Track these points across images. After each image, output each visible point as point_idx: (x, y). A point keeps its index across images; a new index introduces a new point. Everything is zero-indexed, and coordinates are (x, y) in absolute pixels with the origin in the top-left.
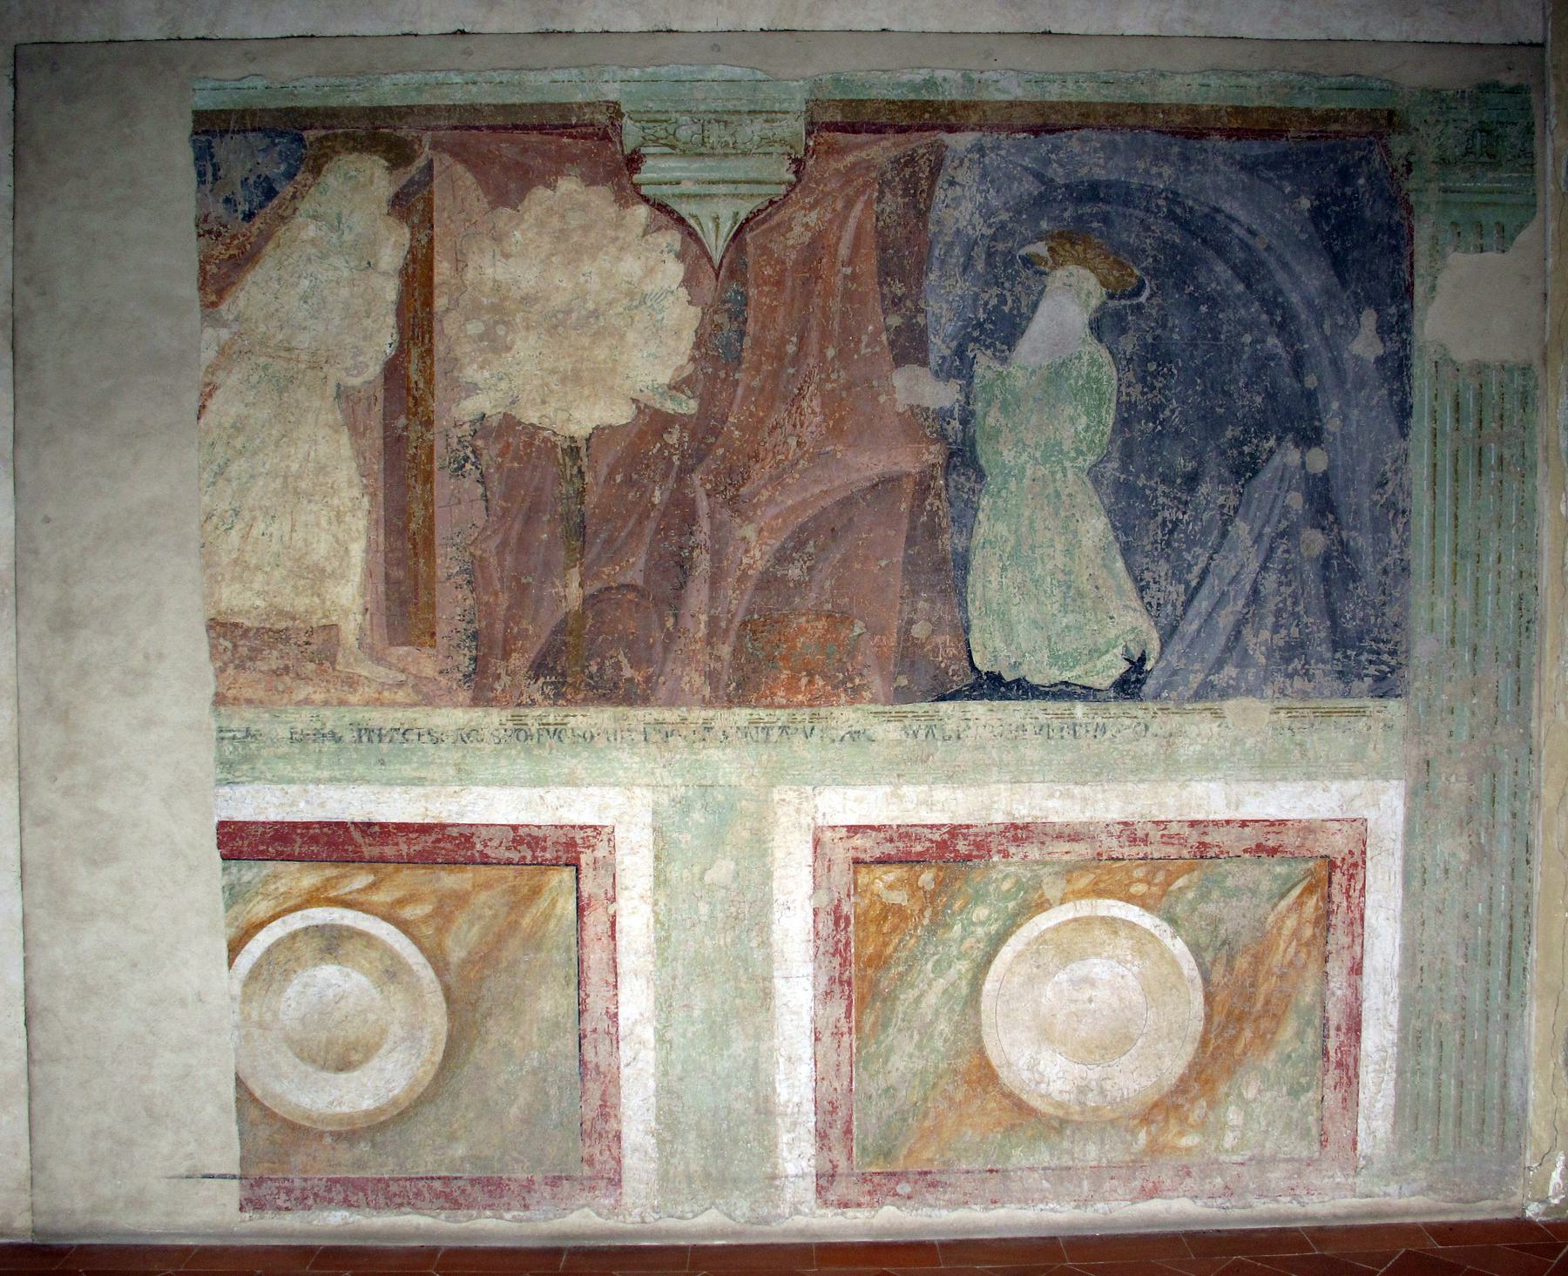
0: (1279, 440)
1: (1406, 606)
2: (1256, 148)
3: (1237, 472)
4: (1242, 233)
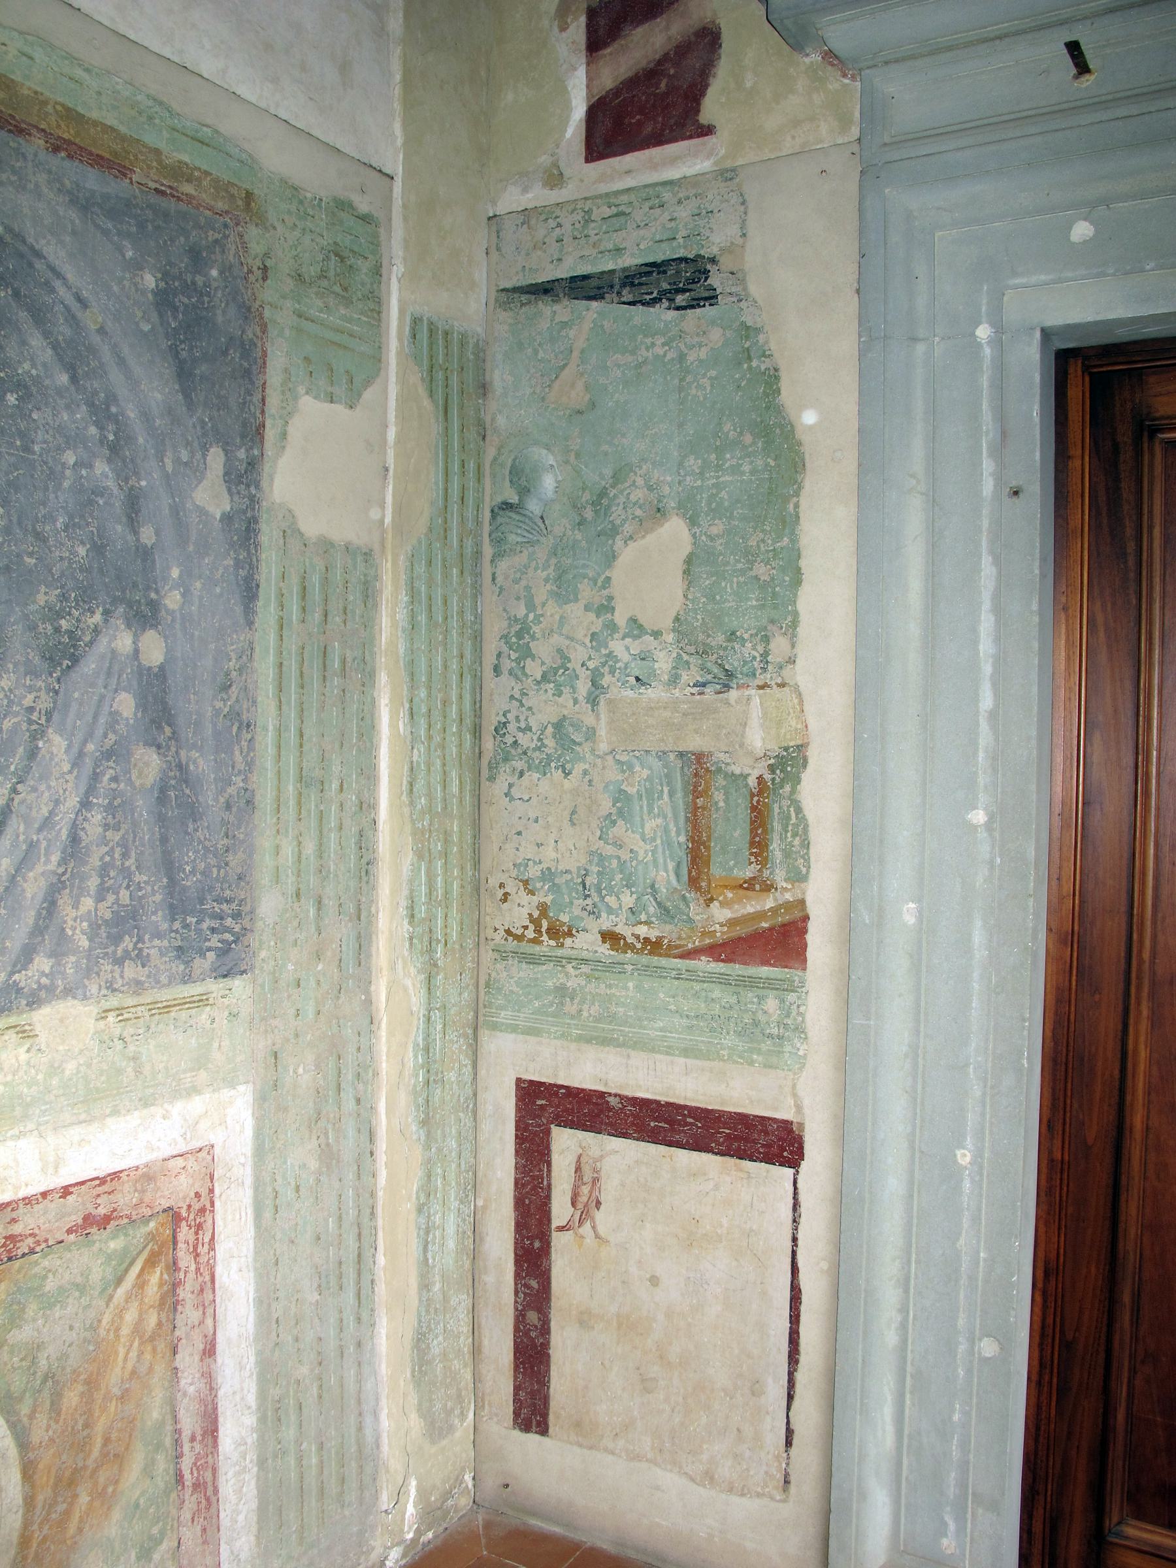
0: (106, 613)
1: (251, 851)
2: (93, 180)
3: (51, 659)
4: (70, 300)
